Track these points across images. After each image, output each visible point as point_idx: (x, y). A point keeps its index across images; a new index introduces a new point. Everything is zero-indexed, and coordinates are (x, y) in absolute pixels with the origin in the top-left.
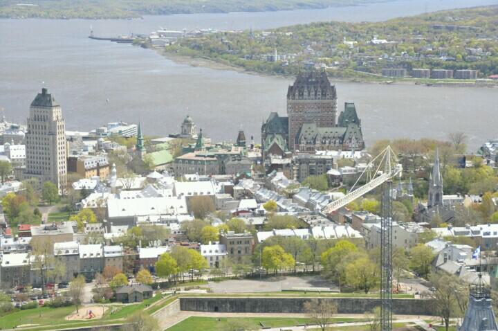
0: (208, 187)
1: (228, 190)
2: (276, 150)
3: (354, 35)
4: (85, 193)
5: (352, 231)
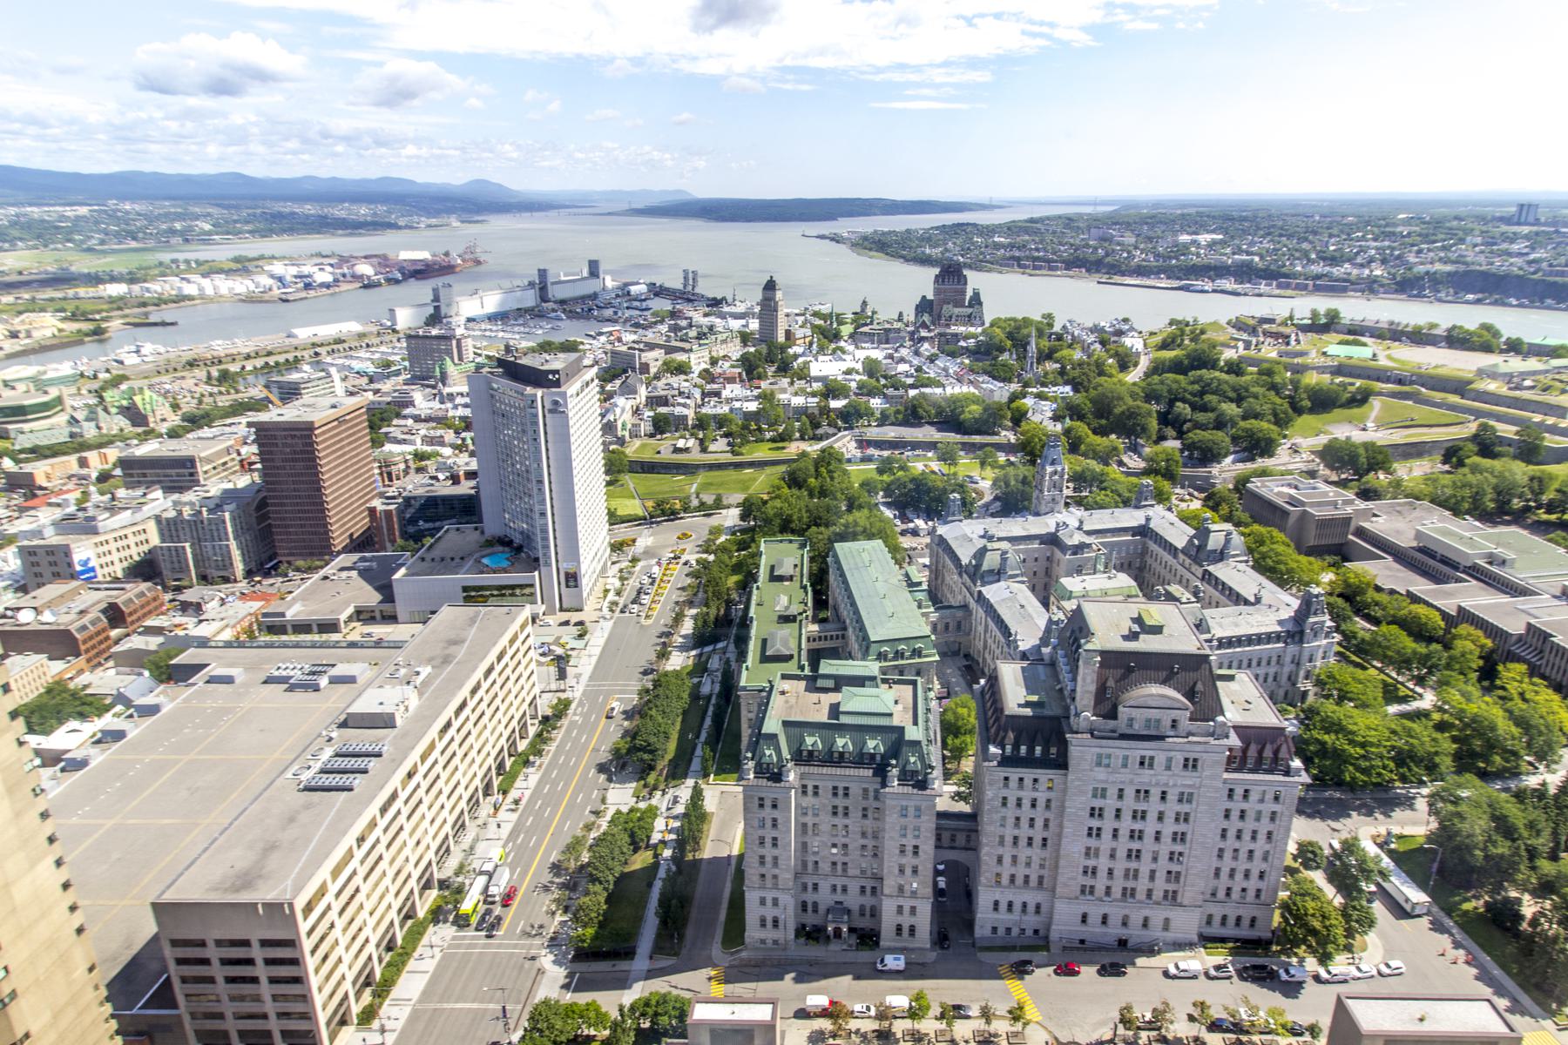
0: (878, 354)
1: (890, 357)
2: (924, 325)
3: (981, 234)
4: (796, 357)
5: (972, 390)
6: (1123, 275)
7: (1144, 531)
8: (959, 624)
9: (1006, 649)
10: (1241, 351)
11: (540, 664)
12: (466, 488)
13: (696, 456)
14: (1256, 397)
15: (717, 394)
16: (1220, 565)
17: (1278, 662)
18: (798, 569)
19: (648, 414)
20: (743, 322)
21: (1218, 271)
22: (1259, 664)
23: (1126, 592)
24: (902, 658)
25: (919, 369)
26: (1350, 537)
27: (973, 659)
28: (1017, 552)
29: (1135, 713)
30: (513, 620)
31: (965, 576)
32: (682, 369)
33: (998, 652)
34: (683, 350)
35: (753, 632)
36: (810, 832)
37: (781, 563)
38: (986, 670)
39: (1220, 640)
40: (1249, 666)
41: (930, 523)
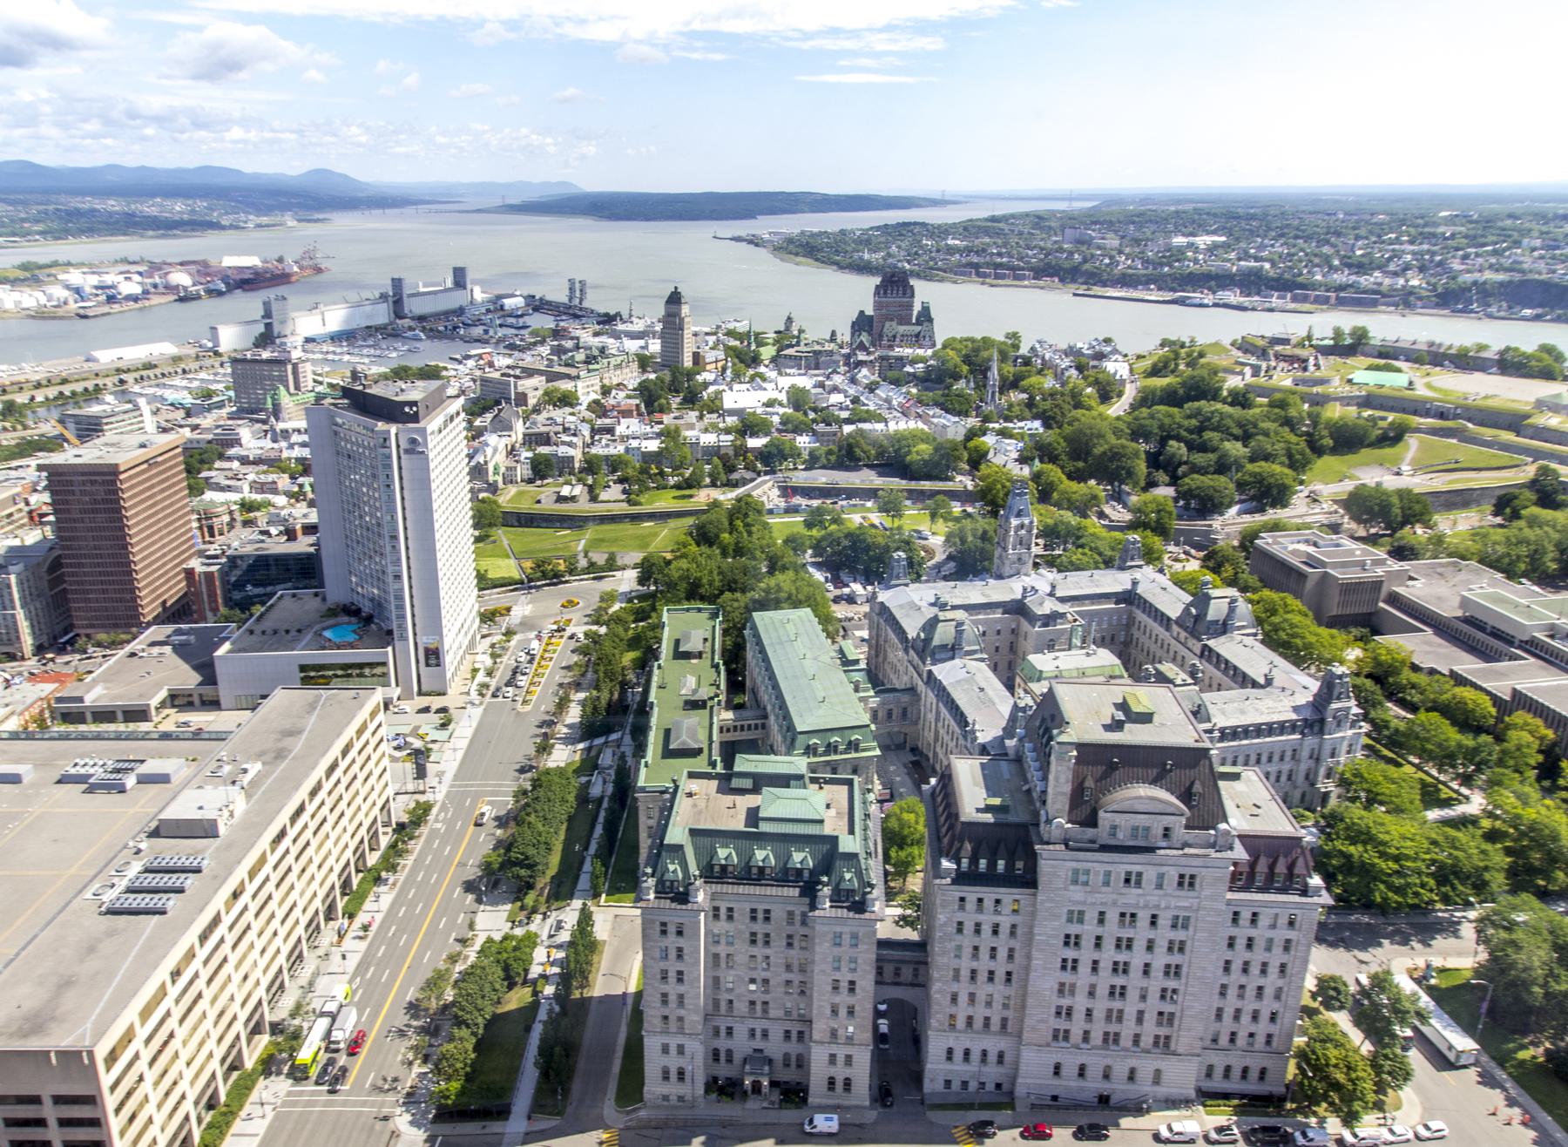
0: (805, 382)
1: (821, 385)
2: (862, 347)
3: (931, 236)
4: (706, 385)
5: (921, 425)
6: (1105, 285)
7: (1129, 598)
8: (904, 712)
9: (961, 741)
10: (1249, 379)
11: (394, 759)
12: (303, 545)
13: (584, 506)
14: (1267, 434)
15: (610, 430)
16: (1222, 639)
17: (1293, 757)
18: (708, 644)
19: (526, 454)
20: (641, 343)
21: (1219, 281)
22: (1270, 760)
23: (1108, 672)
24: (836, 752)
25: (855, 400)
26: (1381, 605)
27: (921, 754)
28: (976, 623)
29: (1119, 819)
30: (361, 706)
31: (912, 652)
32: (567, 400)
33: (952, 745)
34: (568, 377)
35: (654, 721)
36: (723, 965)
37: (687, 636)
38: (938, 767)
39: (1222, 730)
40: (1258, 762)
41: (869, 588)
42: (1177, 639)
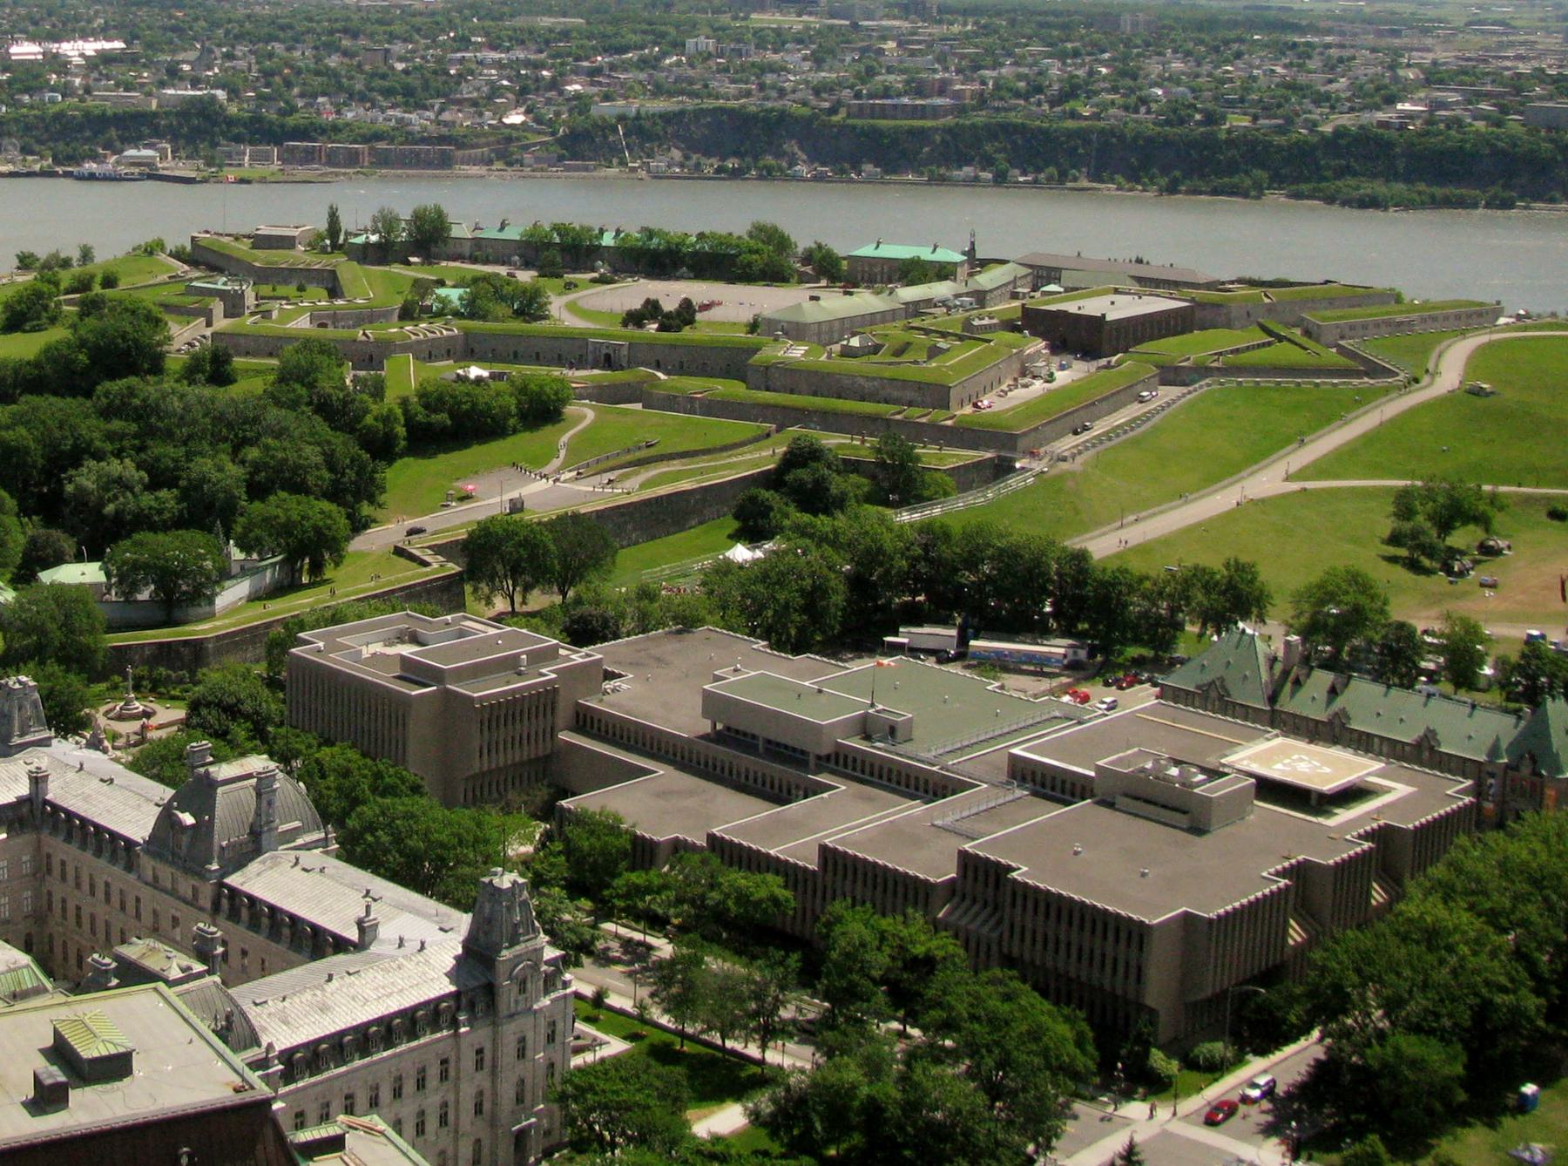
10: (221, 323)
14: (279, 434)
16: (254, 867)
17: (444, 1076)
22: (397, 1093)
26: (564, 736)
39: (287, 1056)
42: (155, 883)
